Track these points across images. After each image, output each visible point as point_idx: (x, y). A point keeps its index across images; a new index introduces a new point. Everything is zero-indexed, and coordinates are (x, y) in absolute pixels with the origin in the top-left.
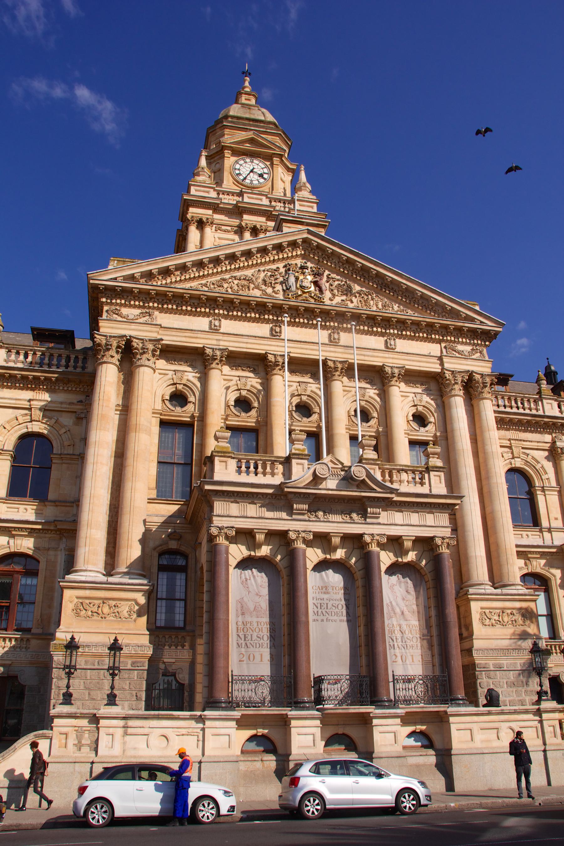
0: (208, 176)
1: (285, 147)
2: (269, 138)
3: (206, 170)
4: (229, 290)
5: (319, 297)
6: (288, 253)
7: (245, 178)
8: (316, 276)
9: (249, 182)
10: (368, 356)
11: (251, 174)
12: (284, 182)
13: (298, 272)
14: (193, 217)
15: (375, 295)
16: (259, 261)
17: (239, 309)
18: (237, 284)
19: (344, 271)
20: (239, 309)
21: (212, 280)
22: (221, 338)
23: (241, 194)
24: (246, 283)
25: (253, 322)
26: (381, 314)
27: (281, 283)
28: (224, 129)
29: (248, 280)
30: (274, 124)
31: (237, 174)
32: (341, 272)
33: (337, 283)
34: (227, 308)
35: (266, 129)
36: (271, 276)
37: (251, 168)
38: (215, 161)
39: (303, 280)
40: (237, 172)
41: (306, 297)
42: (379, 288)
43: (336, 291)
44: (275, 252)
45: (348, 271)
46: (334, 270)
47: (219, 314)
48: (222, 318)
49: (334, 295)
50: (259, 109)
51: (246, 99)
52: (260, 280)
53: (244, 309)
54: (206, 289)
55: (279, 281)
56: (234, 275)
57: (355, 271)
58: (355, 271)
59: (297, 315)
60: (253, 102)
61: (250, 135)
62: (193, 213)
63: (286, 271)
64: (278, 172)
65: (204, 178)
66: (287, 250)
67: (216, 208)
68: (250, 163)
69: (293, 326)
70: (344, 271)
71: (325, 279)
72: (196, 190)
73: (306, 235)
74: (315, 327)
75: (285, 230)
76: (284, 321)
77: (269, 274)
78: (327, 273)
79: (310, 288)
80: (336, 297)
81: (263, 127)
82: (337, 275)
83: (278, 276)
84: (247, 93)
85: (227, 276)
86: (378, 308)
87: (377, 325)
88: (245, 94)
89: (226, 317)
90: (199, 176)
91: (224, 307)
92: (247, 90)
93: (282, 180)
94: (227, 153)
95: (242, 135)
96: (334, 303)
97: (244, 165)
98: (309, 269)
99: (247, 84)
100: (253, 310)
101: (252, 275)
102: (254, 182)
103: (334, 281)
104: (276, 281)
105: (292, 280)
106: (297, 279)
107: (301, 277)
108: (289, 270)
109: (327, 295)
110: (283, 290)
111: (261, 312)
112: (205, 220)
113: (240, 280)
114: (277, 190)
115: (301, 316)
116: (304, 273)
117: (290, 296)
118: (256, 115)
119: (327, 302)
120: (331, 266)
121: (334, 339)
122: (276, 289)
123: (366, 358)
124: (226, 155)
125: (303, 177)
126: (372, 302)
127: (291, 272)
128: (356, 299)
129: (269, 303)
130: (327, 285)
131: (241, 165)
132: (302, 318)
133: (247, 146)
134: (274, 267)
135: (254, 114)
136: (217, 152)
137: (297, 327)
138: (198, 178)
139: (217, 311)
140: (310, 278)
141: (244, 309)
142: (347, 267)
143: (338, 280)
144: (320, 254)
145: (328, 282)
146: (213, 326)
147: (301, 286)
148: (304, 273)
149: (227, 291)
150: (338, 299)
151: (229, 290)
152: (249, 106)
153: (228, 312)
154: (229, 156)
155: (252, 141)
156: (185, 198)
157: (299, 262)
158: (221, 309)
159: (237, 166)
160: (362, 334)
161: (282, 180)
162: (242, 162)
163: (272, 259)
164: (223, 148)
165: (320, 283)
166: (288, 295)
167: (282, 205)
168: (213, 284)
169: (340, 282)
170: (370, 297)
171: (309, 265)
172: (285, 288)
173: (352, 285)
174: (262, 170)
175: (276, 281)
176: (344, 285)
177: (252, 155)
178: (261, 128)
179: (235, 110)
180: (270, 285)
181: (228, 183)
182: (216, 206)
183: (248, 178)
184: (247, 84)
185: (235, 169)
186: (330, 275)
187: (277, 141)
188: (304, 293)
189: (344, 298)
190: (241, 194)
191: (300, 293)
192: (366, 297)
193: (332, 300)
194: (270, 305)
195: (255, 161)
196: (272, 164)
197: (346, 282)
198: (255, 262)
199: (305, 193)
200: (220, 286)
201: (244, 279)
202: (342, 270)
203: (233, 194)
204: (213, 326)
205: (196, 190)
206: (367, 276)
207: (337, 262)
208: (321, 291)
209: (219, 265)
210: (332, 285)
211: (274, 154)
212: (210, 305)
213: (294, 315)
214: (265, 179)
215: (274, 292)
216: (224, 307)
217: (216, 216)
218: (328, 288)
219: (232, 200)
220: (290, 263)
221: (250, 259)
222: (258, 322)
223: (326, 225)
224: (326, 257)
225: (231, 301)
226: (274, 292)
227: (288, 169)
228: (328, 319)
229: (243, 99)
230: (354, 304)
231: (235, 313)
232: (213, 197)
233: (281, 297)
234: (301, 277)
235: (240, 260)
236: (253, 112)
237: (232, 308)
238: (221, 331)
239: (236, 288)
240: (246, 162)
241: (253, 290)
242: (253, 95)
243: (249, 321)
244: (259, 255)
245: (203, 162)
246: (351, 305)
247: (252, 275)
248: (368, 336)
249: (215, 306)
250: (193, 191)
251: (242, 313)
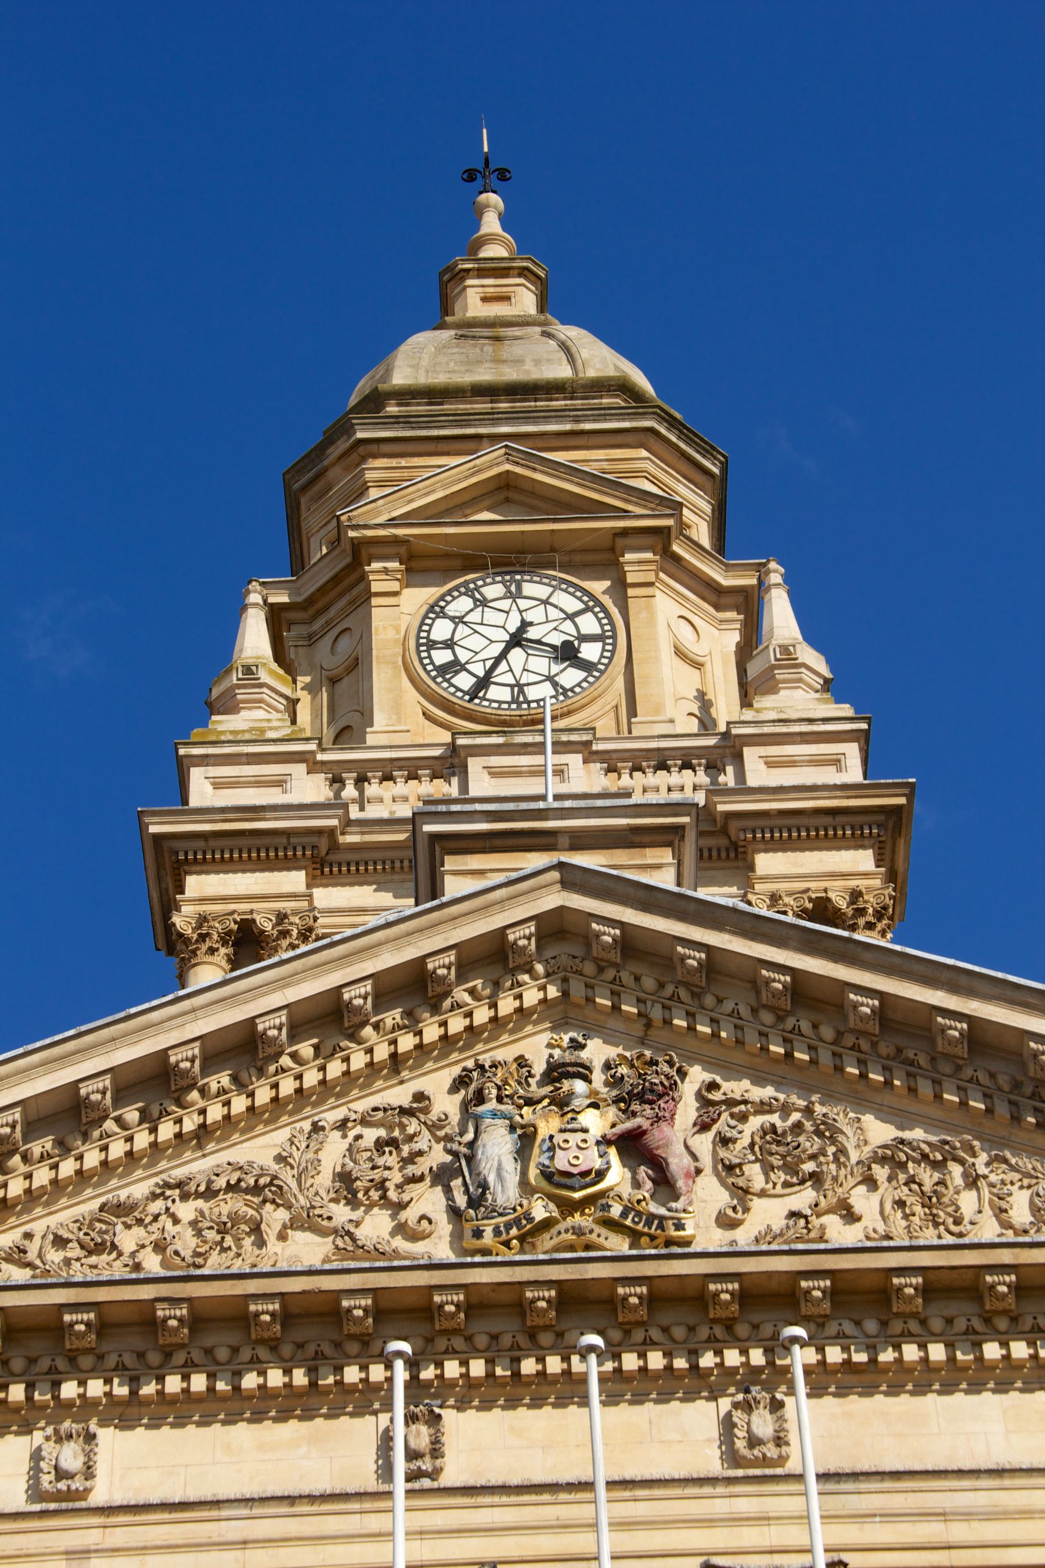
0: (281, 704)
1: (684, 491)
2: (594, 459)
3: (264, 677)
4: (152, 1263)
5: (651, 1217)
6: (470, 1006)
7: (484, 683)
8: (635, 1107)
9: (505, 694)
10: (968, 1516)
11: (517, 655)
12: (698, 665)
13: (530, 1102)
14: (202, 919)
15: (983, 1157)
16: (311, 1078)
17: (197, 1356)
18: (194, 1224)
19: (789, 1055)
20: (197, 1356)
21: (53, 1221)
22: (92, 1538)
23: (452, 763)
24: (229, 1205)
25: (283, 1416)
26: (1006, 1257)
27: (442, 1177)
28: (364, 459)
29: (256, 1189)
30: (624, 387)
31: (444, 670)
32: (775, 1059)
33: (756, 1122)
34: (128, 1359)
35: (577, 420)
36: (380, 1145)
37: (513, 625)
38: (329, 625)
39: (559, 1139)
40: (442, 657)
41: (578, 1231)
42: (1002, 1110)
43: (755, 1175)
44: (393, 1016)
45: (811, 1048)
46: (738, 1057)
47: (86, 1406)
48: (102, 1424)
49: (742, 1194)
50: (545, 334)
51: (485, 299)
52: (324, 1180)
53: (222, 1354)
54: (20, 1275)
55: (423, 1166)
56: (179, 1173)
57: (849, 1040)
58: (849, 1040)
59: (523, 1340)
60: (525, 300)
61: (492, 463)
62: (202, 900)
63: (465, 1106)
64: (652, 621)
65: (260, 714)
66: (461, 994)
67: (323, 855)
68: (505, 604)
69: (512, 1404)
70: (789, 1055)
71: (687, 1110)
72: (218, 785)
73: (553, 899)
74: (570, 1390)
75: (454, 887)
76: (583, 1380)
77: (371, 1135)
78: (697, 1075)
79: (601, 1174)
80: (756, 1203)
81: (558, 415)
82: (759, 1081)
83: (422, 1143)
84: (497, 270)
85: (138, 1189)
86: (1007, 1225)
87: (1002, 1324)
88: (482, 273)
89: (125, 1414)
90: (232, 708)
91: (112, 1360)
92: (493, 251)
93: (680, 653)
94: (382, 572)
95: (449, 475)
96: (743, 1237)
97: (474, 617)
98: (598, 1077)
99: (491, 224)
100: (273, 1345)
101: (280, 1159)
102: (532, 693)
103: (743, 1118)
104: (411, 1170)
105: (497, 1147)
106: (526, 1139)
107: (548, 1125)
108: (480, 1098)
109: (708, 1195)
110: (454, 1212)
111: (319, 1355)
112: (268, 926)
113: (210, 1193)
114: (658, 709)
115: (546, 1339)
116: (562, 1103)
117: (488, 1238)
118: (528, 366)
119: (702, 1230)
120: (715, 1035)
121: (754, 1442)
122: (410, 1215)
123: (959, 1532)
124: (375, 587)
125: (781, 617)
126: (968, 1202)
127: (492, 1105)
128: (875, 1197)
129: (352, 1292)
130: (703, 1144)
131: (458, 620)
132: (553, 1350)
133: (486, 522)
134: (399, 1095)
135: (519, 361)
136: (336, 580)
137: (537, 1403)
138: (224, 723)
139: (69, 1390)
140: (596, 1123)
141: (222, 1354)
142: (805, 1026)
143: (764, 1107)
144: (649, 983)
145: (703, 1127)
146: (46, 1481)
147: (548, 1175)
148: (562, 1103)
149: (137, 1267)
150: (768, 1214)
151: (152, 1263)
152: (493, 331)
153: (134, 1382)
154: (395, 586)
155: (504, 491)
156: (153, 829)
157: (537, 1047)
158: (94, 1372)
159: (441, 630)
160: (921, 1389)
161: (680, 653)
162: (462, 605)
163: (382, 1052)
164: (359, 554)
165: (655, 1137)
166: (478, 1234)
167: (702, 778)
168: (60, 1242)
169: (775, 1118)
170: (956, 1170)
171: (597, 1052)
172: (461, 1201)
173: (841, 1116)
174: (568, 626)
175: (411, 1170)
176: (798, 1127)
177: (511, 560)
178: (546, 419)
179: (421, 360)
180: (375, 1195)
181: (399, 718)
182: (324, 844)
183: (502, 675)
184: (491, 224)
185: (432, 645)
186: (713, 1086)
187: (646, 469)
188: (568, 1207)
189: (803, 1198)
190: (452, 763)
191: (540, 1210)
192: (928, 1177)
193: (726, 1220)
194: (358, 1306)
195: (528, 589)
196: (620, 588)
197: (808, 1111)
198: (287, 1087)
199: (799, 700)
200: (99, 1248)
201: (230, 1188)
202: (777, 1049)
203: (412, 770)
204: (46, 1481)
206: (923, 1060)
207: (744, 1011)
208: (664, 1183)
209: (86, 1137)
210: (725, 1141)
211: (625, 532)
212: (32, 1361)
213: (506, 1341)
214: (587, 666)
215: (400, 1229)
216: (112, 1360)
217: (326, 897)
218: (706, 1161)
219: (392, 801)
220: (486, 1059)
221: (261, 1072)
222: (308, 1415)
223: (679, 829)
224: (683, 994)
225: (144, 1320)
226: (400, 1229)
227: (716, 596)
228: (704, 1332)
229: (473, 302)
230: (868, 1223)
231: (173, 1384)
232: (308, 799)
233: (441, 1249)
234: (548, 1125)
235: (203, 1092)
236: (515, 350)
237: (154, 1358)
238: (99, 1497)
239: (186, 1243)
240: (483, 603)
241: (282, 1237)
242: (523, 272)
243: (258, 1417)
244: (305, 1048)
245: (255, 638)
246: (839, 1232)
247: (280, 1159)
248: (959, 1399)
249: (61, 1364)
250: (201, 789)
251: (212, 1376)
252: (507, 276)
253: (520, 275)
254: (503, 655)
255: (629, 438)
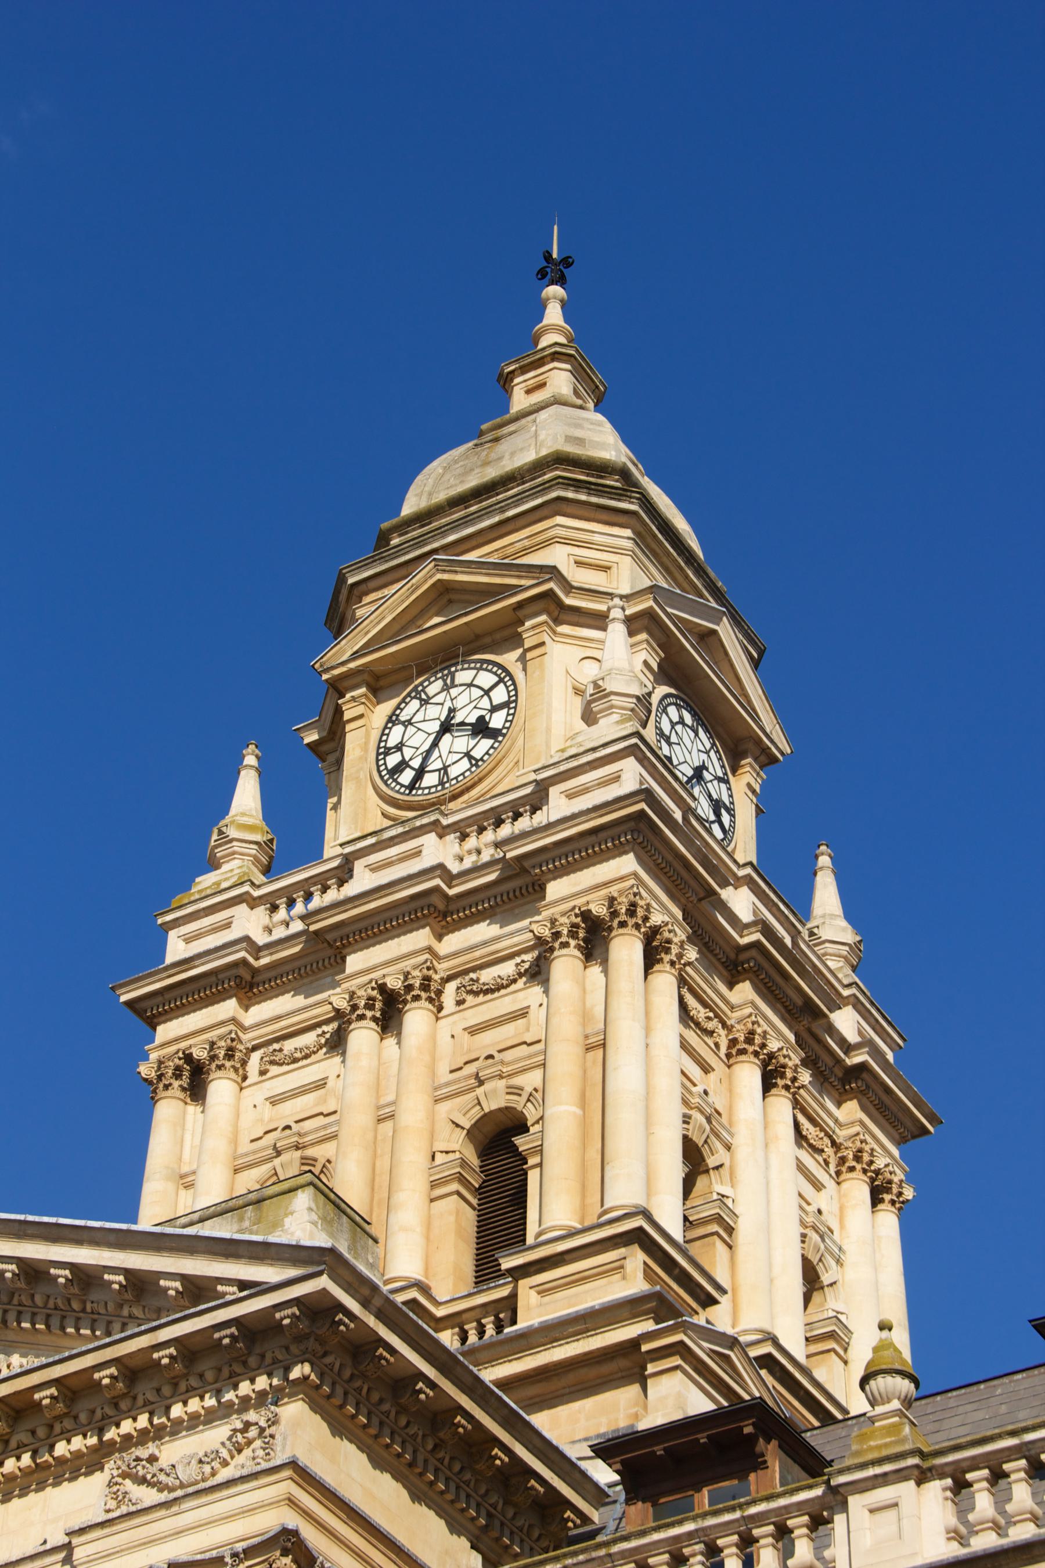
35: (503, 510)
61: (425, 577)
72: (188, 940)
133: (437, 626)
154: (361, 709)
155: (445, 596)
205: (188, 940)
252: (543, 365)
253: (553, 360)
254: (435, 744)
255: (545, 511)
